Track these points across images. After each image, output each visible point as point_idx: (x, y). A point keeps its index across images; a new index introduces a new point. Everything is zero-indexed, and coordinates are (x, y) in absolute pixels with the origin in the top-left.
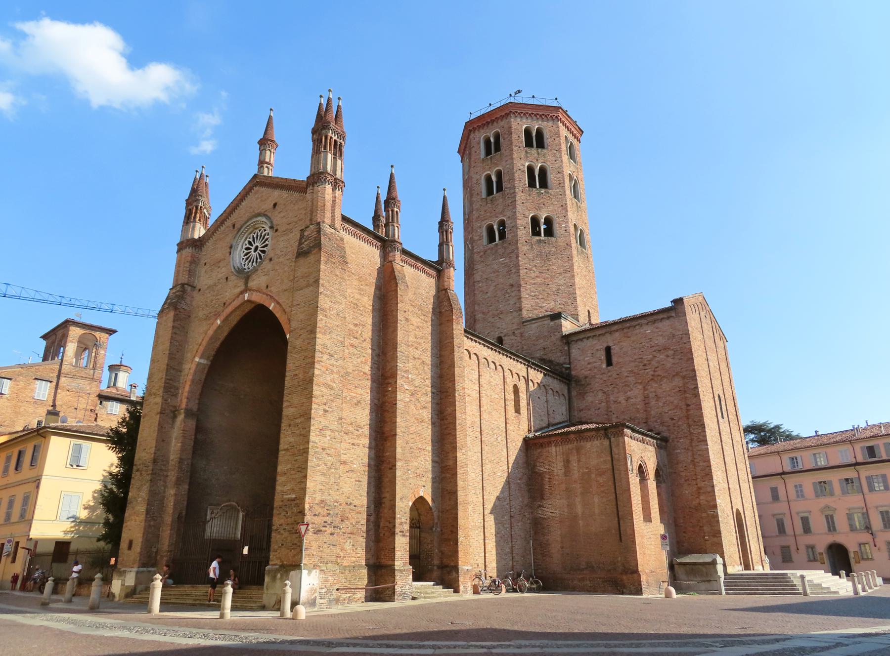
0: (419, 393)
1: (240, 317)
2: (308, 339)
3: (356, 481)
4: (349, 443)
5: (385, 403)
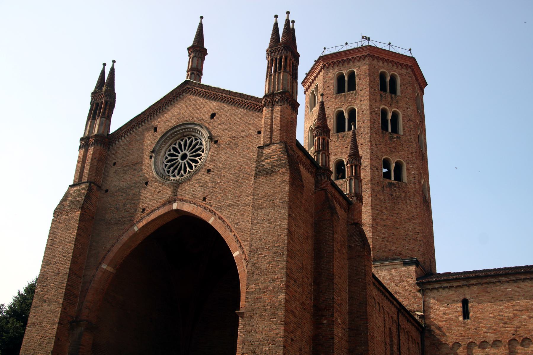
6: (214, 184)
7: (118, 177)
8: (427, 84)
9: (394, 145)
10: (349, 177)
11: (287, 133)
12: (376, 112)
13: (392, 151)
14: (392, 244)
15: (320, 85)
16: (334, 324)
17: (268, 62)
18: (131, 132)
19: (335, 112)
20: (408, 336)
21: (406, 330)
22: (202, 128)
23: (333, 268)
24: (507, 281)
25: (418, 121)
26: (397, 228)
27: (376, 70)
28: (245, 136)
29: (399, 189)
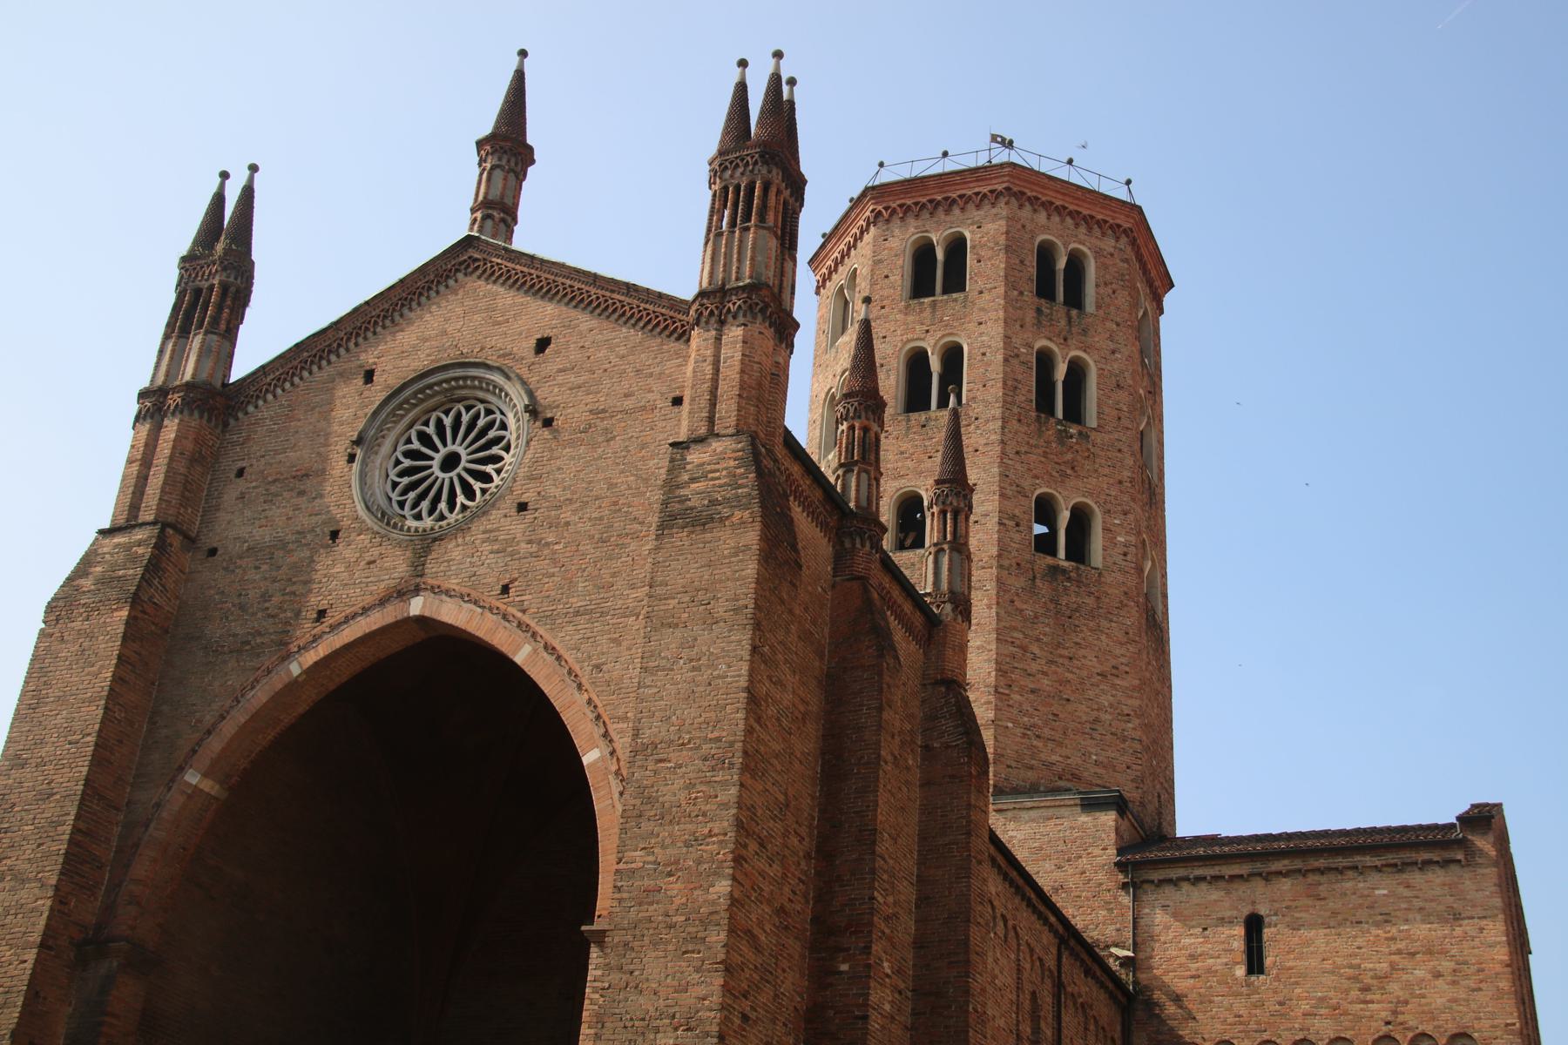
6: (534, 548)
7: (248, 513)
8: (1171, 285)
9: (1069, 456)
10: (935, 545)
11: (757, 406)
12: (1021, 359)
13: (1067, 476)
14: (1050, 745)
15: (864, 272)
16: (872, 974)
17: (714, 195)
18: (296, 380)
19: (902, 356)
20: (1086, 1018)
21: (1081, 1000)
22: (508, 378)
23: (876, 810)
24: (1376, 867)
25: (1141, 391)
26: (1068, 700)
27: (1027, 236)
28: (634, 410)
29: (1079, 587)
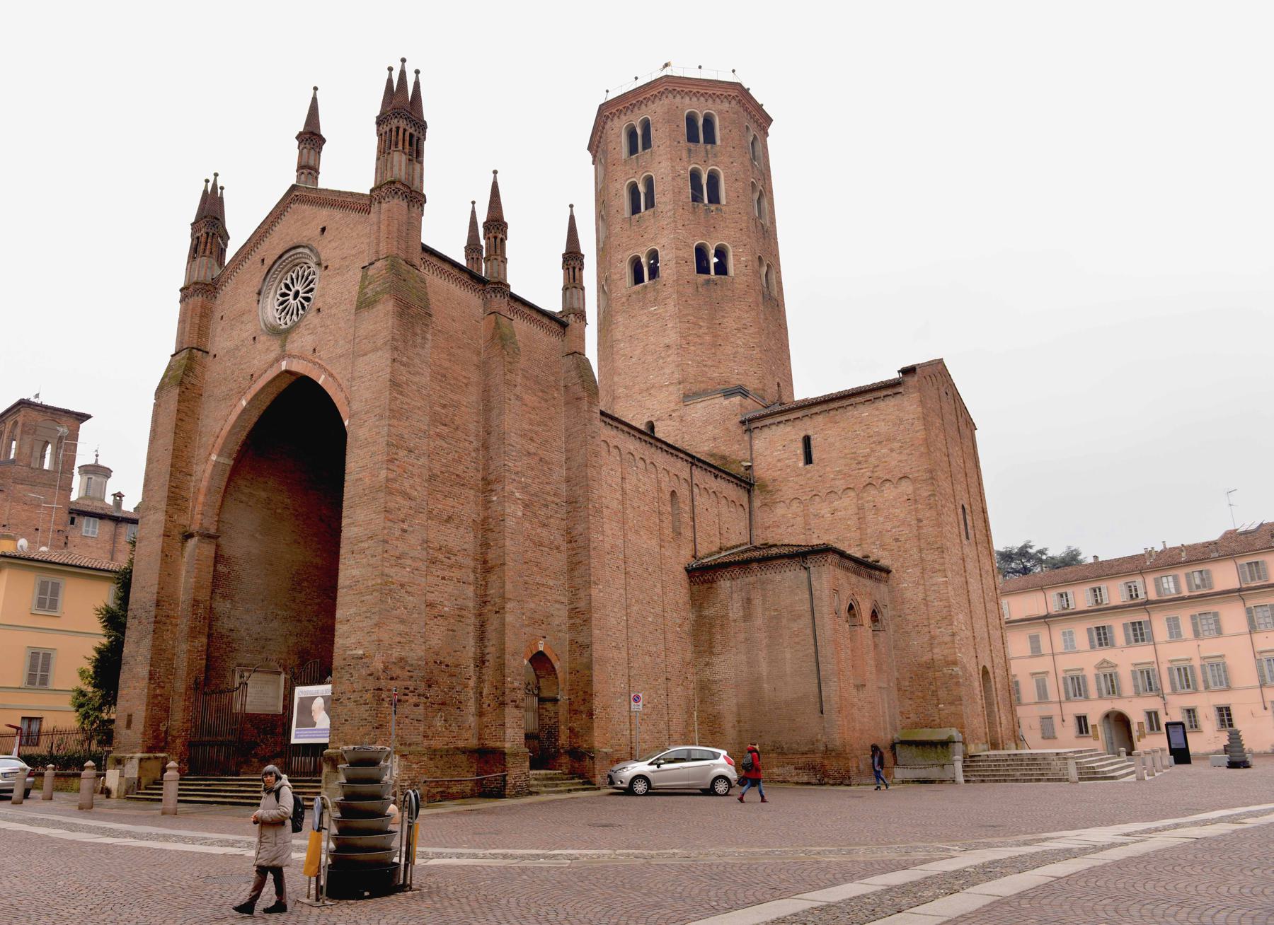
0: (535, 504)
1: (275, 395)
2: (377, 427)
3: (448, 630)
4: (438, 576)
5: (488, 517)
14: (712, 369)
27: (679, 112)
